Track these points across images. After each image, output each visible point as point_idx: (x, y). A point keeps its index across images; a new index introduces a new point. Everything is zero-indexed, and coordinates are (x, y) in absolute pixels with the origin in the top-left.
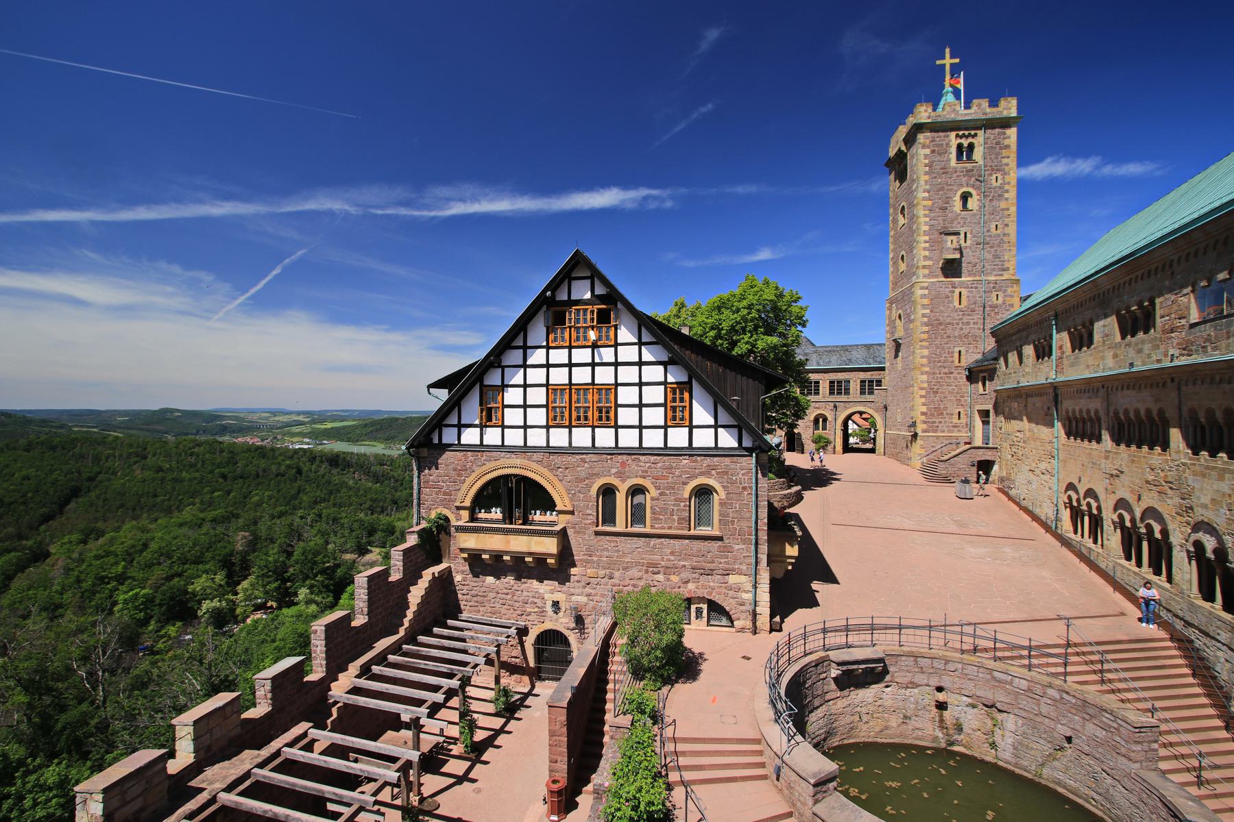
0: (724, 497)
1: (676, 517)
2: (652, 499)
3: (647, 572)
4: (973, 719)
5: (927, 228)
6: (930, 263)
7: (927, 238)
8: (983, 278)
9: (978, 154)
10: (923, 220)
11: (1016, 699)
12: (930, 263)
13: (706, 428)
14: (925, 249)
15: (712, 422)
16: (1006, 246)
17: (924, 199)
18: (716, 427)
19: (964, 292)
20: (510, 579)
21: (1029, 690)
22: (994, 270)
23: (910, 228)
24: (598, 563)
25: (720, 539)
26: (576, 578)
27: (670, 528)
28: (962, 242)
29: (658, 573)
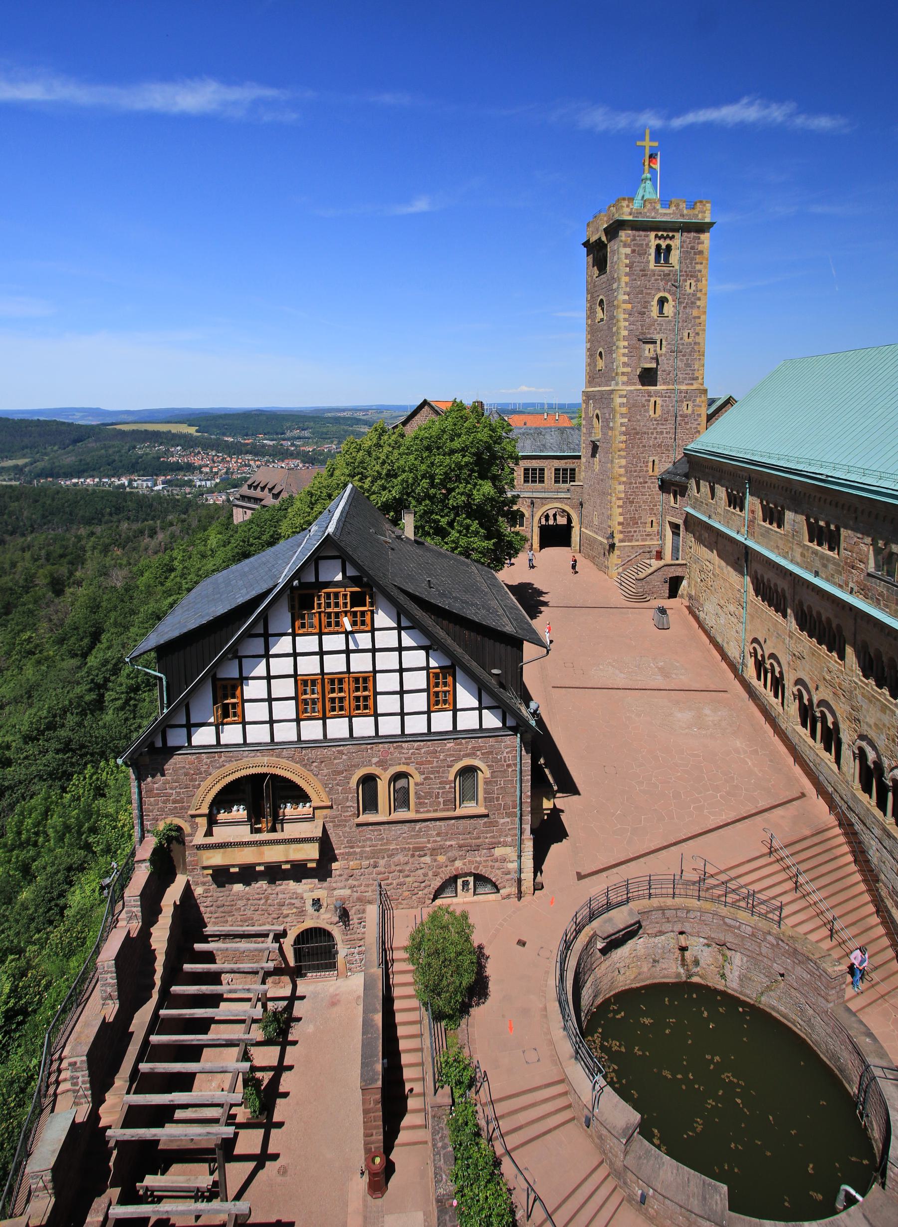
0: (488, 775)
1: (441, 800)
2: (416, 784)
3: (413, 856)
4: (707, 956)
6: (629, 370)
7: (626, 344)
8: (677, 387)
10: (623, 324)
11: (743, 940)
12: (629, 370)
13: (469, 710)
14: (624, 355)
15: (476, 704)
18: (480, 709)
20: (263, 884)
22: (685, 379)
23: (610, 329)
24: (362, 852)
25: (487, 816)
26: (338, 872)
27: (435, 811)
29: (425, 855)
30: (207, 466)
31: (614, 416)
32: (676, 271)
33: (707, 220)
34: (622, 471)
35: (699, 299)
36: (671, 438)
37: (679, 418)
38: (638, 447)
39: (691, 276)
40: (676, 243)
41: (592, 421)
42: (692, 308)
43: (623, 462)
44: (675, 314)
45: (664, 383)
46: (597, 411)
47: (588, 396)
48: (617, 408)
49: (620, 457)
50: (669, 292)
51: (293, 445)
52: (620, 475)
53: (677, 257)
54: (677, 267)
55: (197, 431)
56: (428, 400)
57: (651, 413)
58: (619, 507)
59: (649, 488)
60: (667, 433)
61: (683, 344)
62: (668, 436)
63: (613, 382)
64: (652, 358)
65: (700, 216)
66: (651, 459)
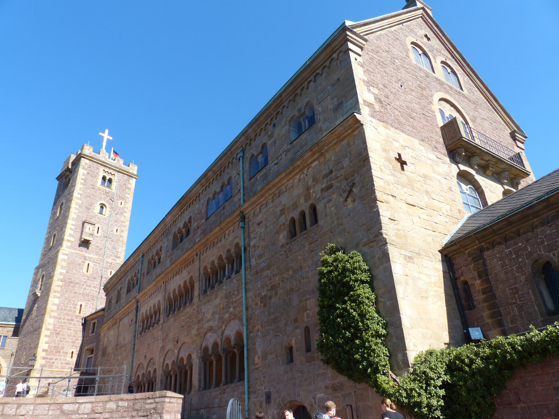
5: (75, 216)
6: (73, 239)
9: (114, 184)
12: (73, 239)
14: (71, 229)
16: (120, 243)
21: (93, 411)
22: (111, 256)
28: (96, 232)
33: (135, 173)
34: (55, 308)
35: (126, 212)
36: (96, 291)
38: (71, 292)
43: (57, 301)
44: (110, 216)
46: (44, 273)
49: (55, 297)
50: (108, 202)
52: (52, 311)
58: (46, 336)
59: (74, 325)
62: (95, 290)
64: (90, 234)
66: (79, 303)
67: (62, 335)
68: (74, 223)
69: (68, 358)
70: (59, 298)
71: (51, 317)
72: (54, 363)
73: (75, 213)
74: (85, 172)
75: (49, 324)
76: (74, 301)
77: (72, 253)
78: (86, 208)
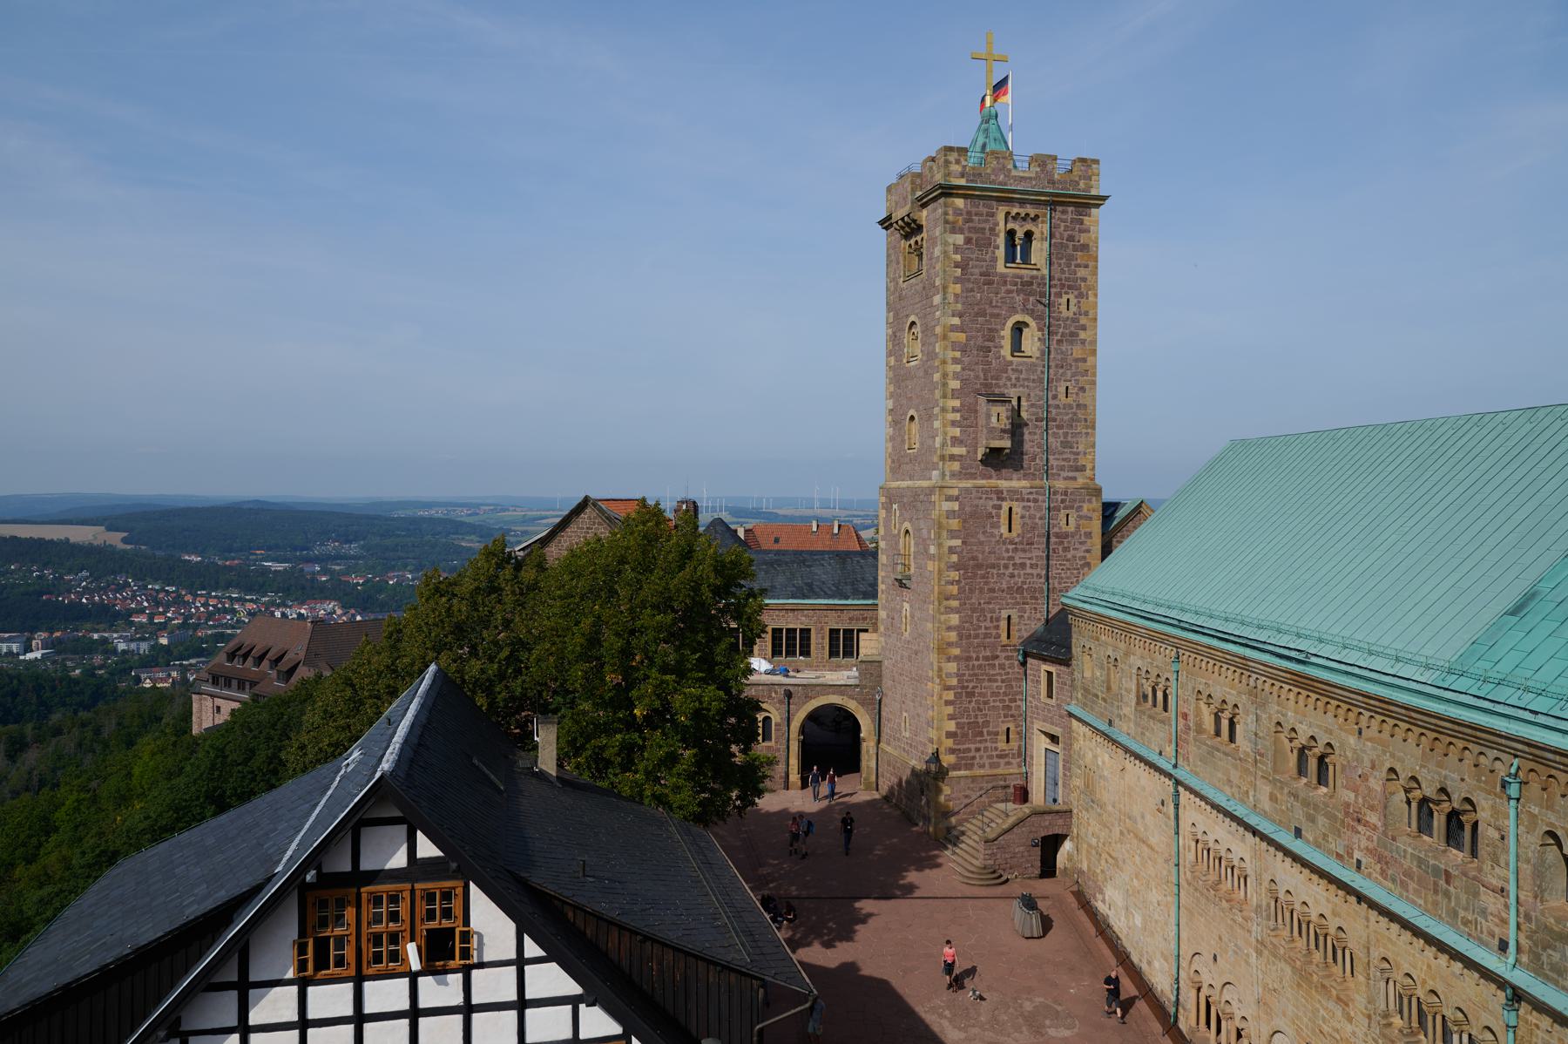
5: (955, 384)
14: (954, 423)
17: (954, 328)
19: (1018, 508)
22: (1062, 468)
30: (142, 611)
31: (939, 536)
32: (1043, 278)
34: (953, 636)
35: (1084, 328)
36: (1039, 576)
37: (1053, 540)
38: (981, 590)
39: (1070, 287)
40: (1041, 229)
41: (897, 543)
42: (1071, 343)
43: (955, 619)
44: (1043, 353)
45: (1025, 477)
46: (907, 525)
47: (891, 497)
48: (944, 521)
49: (950, 610)
50: (1031, 313)
51: (324, 571)
52: (950, 644)
53: (1045, 254)
54: (1046, 272)
55: (125, 541)
56: (594, 495)
57: (1004, 529)
58: (948, 703)
59: (1002, 667)
60: (1032, 566)
61: (1057, 407)
62: (1035, 572)
63: (935, 473)
64: (1003, 431)
65: (1082, 185)
66: (1004, 614)
67: (980, 694)
68: (957, 403)
69: (1002, 745)
70: (957, 611)
71: (949, 660)
72: (974, 758)
73: (956, 376)
74: (959, 239)
75: (949, 675)
76: (993, 611)
77: (967, 489)
78: (981, 348)
